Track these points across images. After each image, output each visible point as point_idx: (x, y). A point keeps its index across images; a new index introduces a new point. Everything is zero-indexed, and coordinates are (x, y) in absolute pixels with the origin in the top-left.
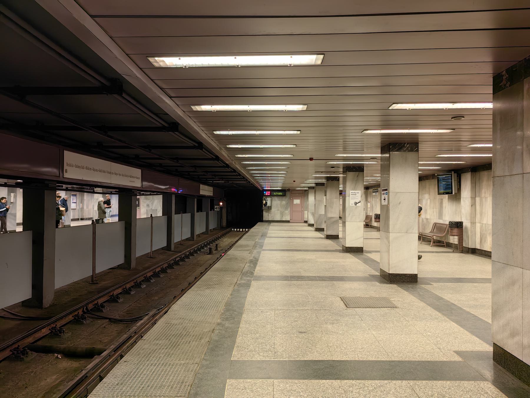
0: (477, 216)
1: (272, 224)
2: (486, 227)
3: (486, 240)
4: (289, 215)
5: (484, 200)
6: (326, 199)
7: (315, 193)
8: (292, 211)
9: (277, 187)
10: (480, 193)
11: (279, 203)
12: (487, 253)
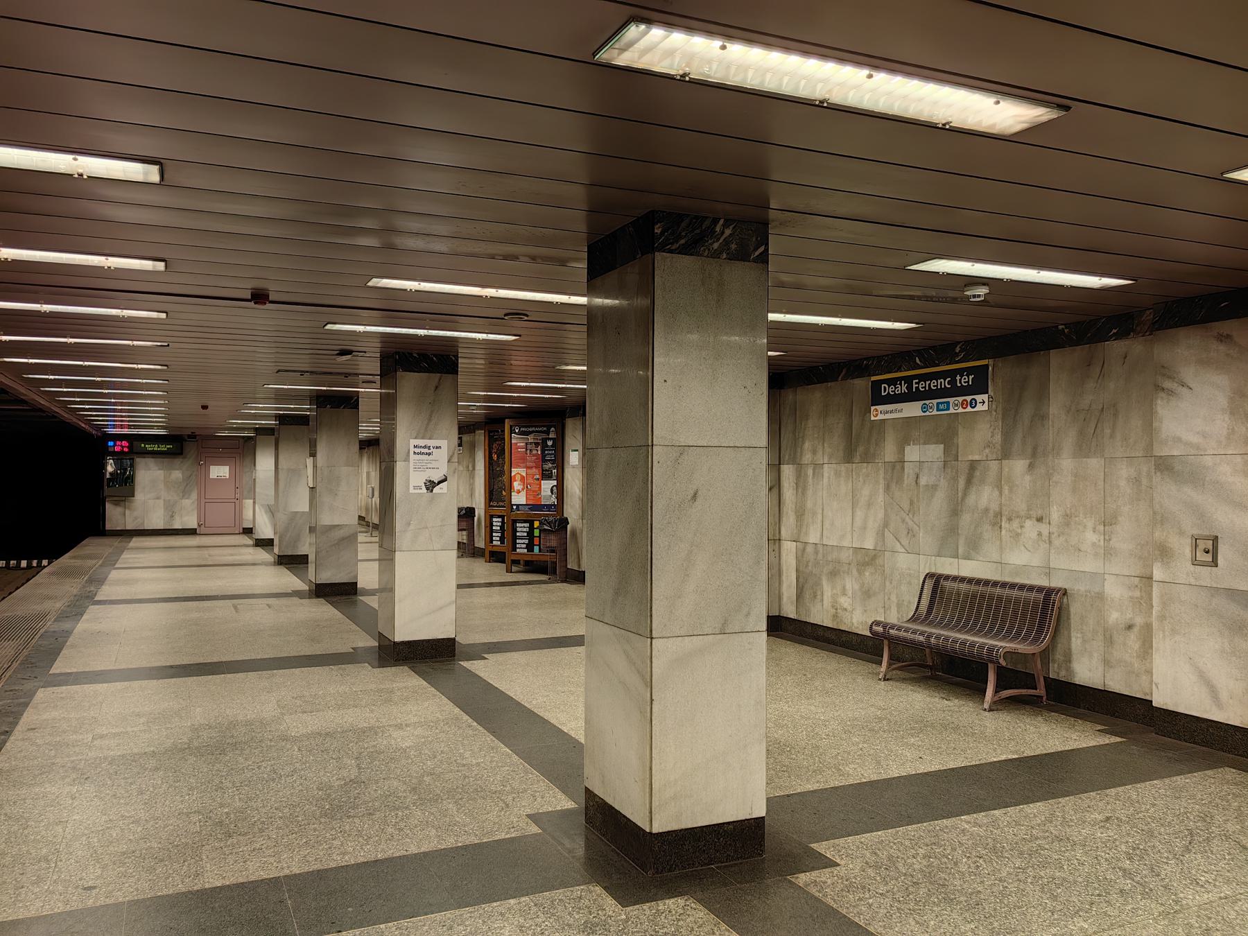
0: (784, 519)
1: (136, 542)
2: (816, 553)
3: (819, 593)
4: (195, 513)
5: (810, 472)
6: (315, 466)
7: (277, 449)
8: (203, 501)
9: (152, 427)
10: (795, 453)
11: (162, 478)
12: (820, 633)
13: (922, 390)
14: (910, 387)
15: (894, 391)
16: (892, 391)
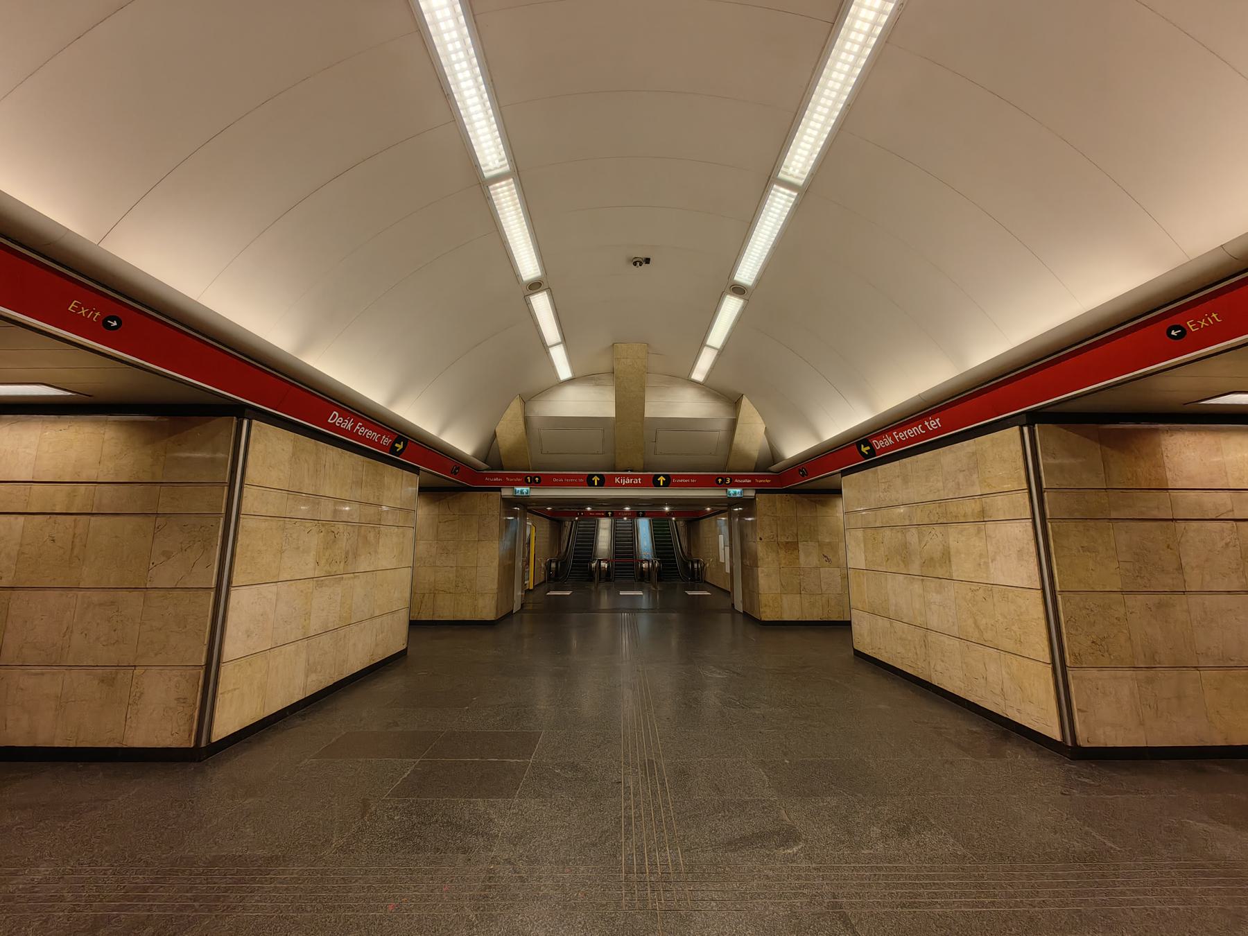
13: (360, 434)
14: (353, 427)
15: (341, 424)
16: (338, 423)
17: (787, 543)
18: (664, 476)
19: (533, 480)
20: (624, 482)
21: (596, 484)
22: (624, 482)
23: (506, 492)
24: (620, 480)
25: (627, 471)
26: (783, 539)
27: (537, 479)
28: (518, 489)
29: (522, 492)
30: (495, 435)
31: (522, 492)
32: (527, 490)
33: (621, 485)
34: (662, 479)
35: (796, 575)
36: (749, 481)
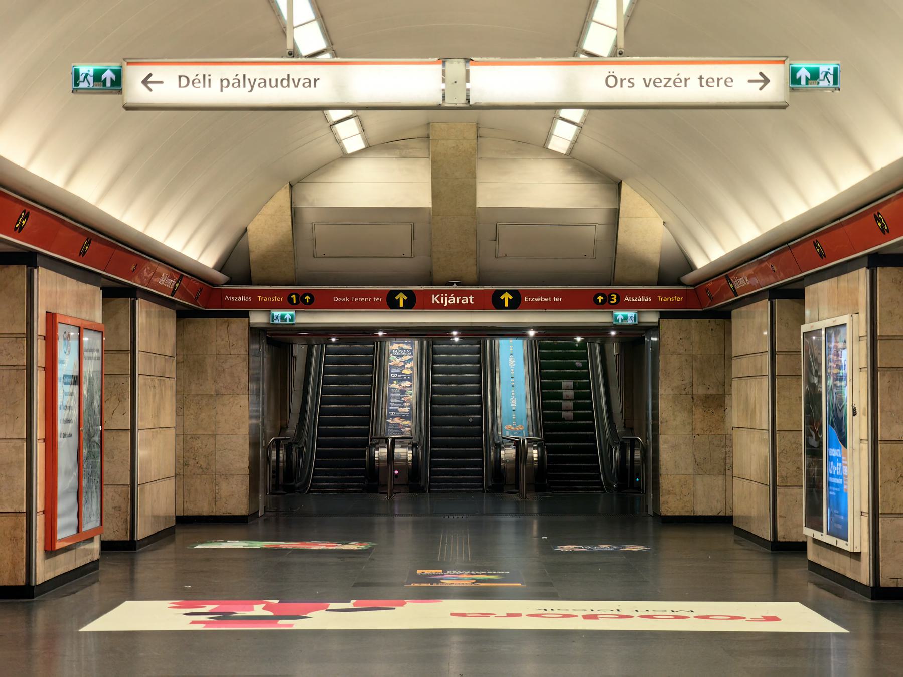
17: (707, 397)
18: (510, 292)
19: (301, 298)
20: (445, 302)
21: (401, 305)
22: (445, 302)
23: (258, 318)
24: (439, 299)
25: (451, 284)
26: (700, 391)
27: (307, 298)
28: (277, 313)
29: (283, 318)
30: (246, 229)
31: (283, 318)
32: (292, 316)
33: (439, 307)
34: (506, 297)
35: (718, 446)
36: (647, 299)
